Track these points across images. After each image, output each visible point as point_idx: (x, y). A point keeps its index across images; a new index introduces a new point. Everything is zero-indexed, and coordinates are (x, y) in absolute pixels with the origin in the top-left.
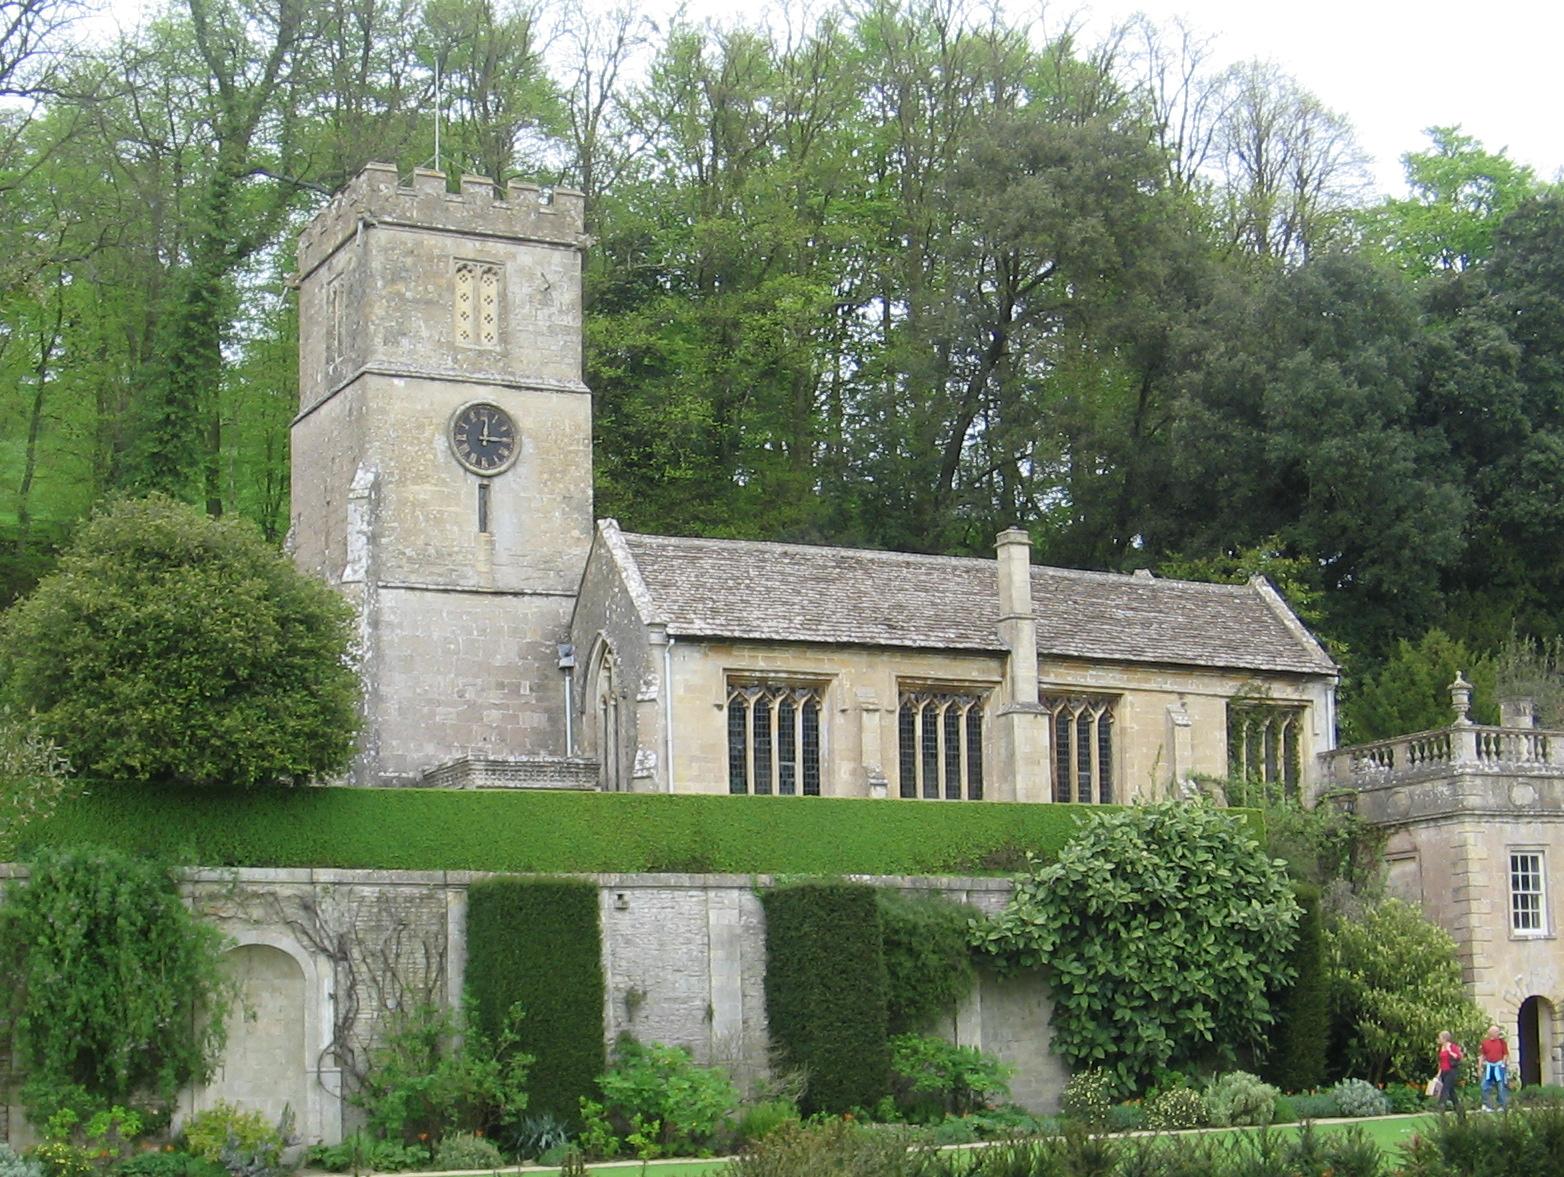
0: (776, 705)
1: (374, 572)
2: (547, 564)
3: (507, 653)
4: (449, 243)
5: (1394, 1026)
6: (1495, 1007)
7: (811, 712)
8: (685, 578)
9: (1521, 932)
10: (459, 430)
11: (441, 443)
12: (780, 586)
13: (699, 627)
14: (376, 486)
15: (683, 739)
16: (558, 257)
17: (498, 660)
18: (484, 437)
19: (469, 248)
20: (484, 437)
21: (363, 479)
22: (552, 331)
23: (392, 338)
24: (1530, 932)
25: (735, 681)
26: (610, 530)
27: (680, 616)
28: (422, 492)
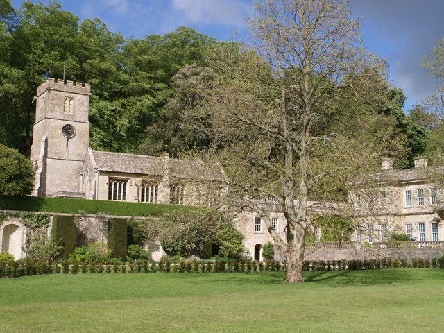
0: (122, 184)
1: (45, 156)
2: (79, 155)
3: (70, 171)
4: (64, 94)
5: (227, 248)
6: (249, 247)
7: (125, 185)
8: (103, 160)
9: (257, 232)
10: (63, 129)
11: (60, 131)
12: (121, 161)
13: (104, 169)
14: (47, 139)
15: (99, 189)
16: (85, 97)
17: (69, 172)
18: (68, 131)
19: (68, 95)
20: (68, 131)
21: (45, 137)
22: (83, 111)
23: (52, 111)
24: (258, 232)
25: (110, 179)
26: (90, 150)
27: (101, 167)
28: (56, 140)
